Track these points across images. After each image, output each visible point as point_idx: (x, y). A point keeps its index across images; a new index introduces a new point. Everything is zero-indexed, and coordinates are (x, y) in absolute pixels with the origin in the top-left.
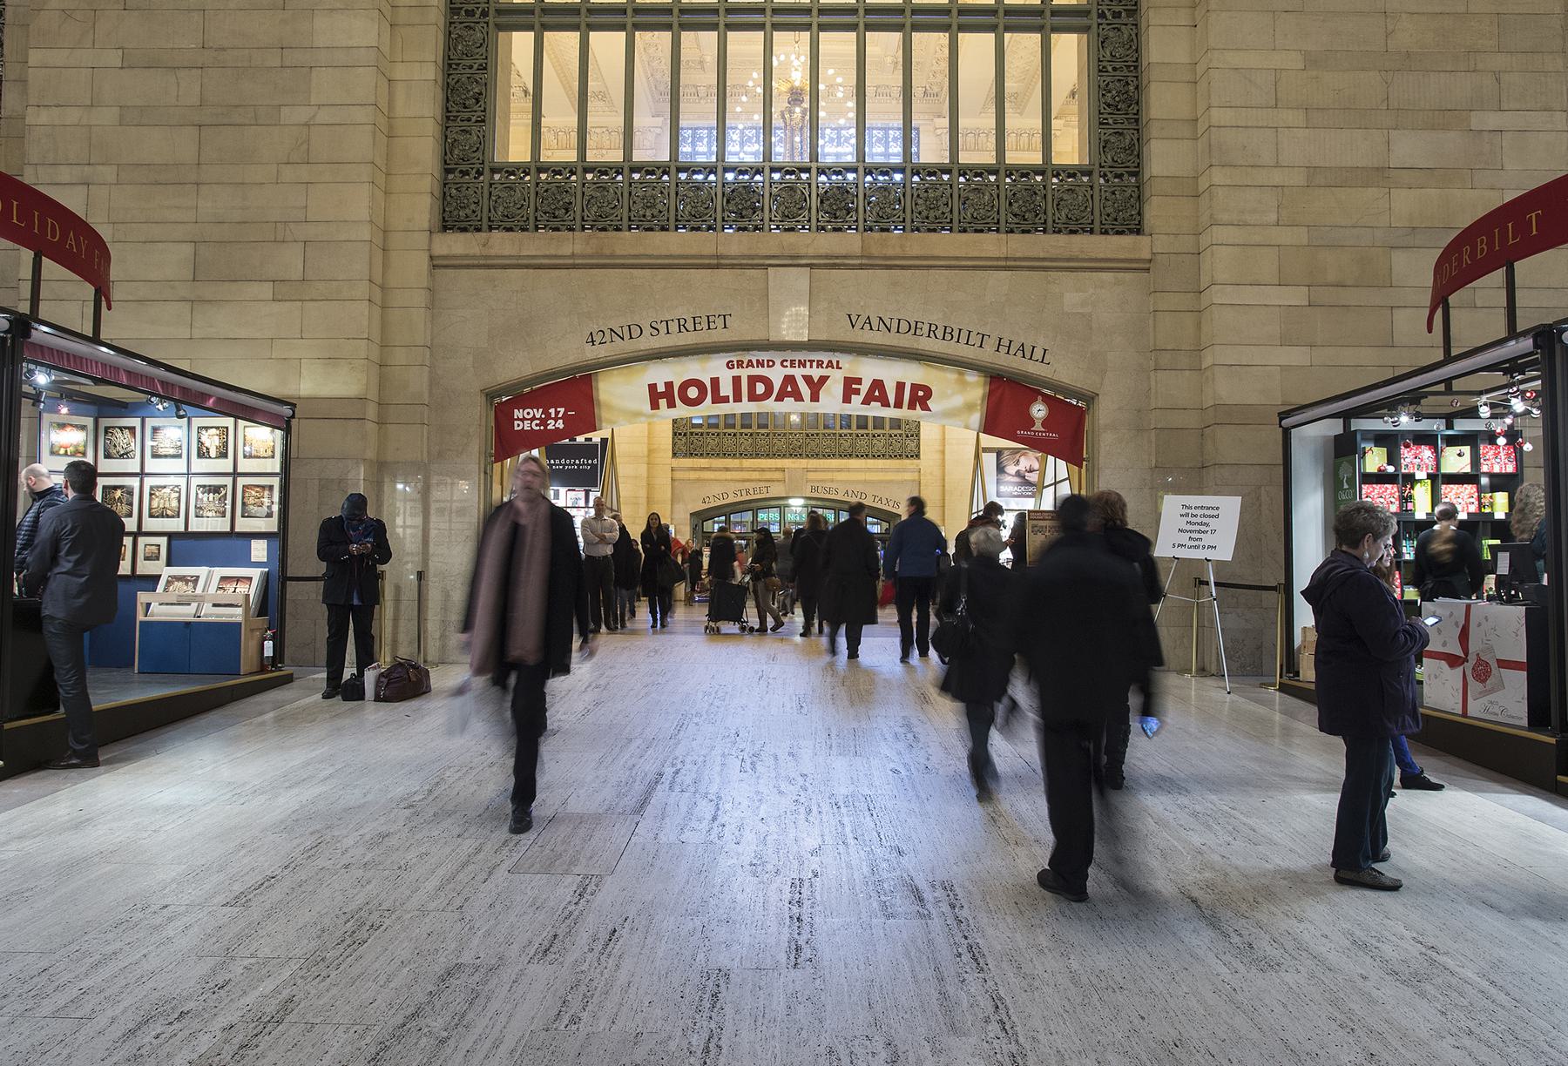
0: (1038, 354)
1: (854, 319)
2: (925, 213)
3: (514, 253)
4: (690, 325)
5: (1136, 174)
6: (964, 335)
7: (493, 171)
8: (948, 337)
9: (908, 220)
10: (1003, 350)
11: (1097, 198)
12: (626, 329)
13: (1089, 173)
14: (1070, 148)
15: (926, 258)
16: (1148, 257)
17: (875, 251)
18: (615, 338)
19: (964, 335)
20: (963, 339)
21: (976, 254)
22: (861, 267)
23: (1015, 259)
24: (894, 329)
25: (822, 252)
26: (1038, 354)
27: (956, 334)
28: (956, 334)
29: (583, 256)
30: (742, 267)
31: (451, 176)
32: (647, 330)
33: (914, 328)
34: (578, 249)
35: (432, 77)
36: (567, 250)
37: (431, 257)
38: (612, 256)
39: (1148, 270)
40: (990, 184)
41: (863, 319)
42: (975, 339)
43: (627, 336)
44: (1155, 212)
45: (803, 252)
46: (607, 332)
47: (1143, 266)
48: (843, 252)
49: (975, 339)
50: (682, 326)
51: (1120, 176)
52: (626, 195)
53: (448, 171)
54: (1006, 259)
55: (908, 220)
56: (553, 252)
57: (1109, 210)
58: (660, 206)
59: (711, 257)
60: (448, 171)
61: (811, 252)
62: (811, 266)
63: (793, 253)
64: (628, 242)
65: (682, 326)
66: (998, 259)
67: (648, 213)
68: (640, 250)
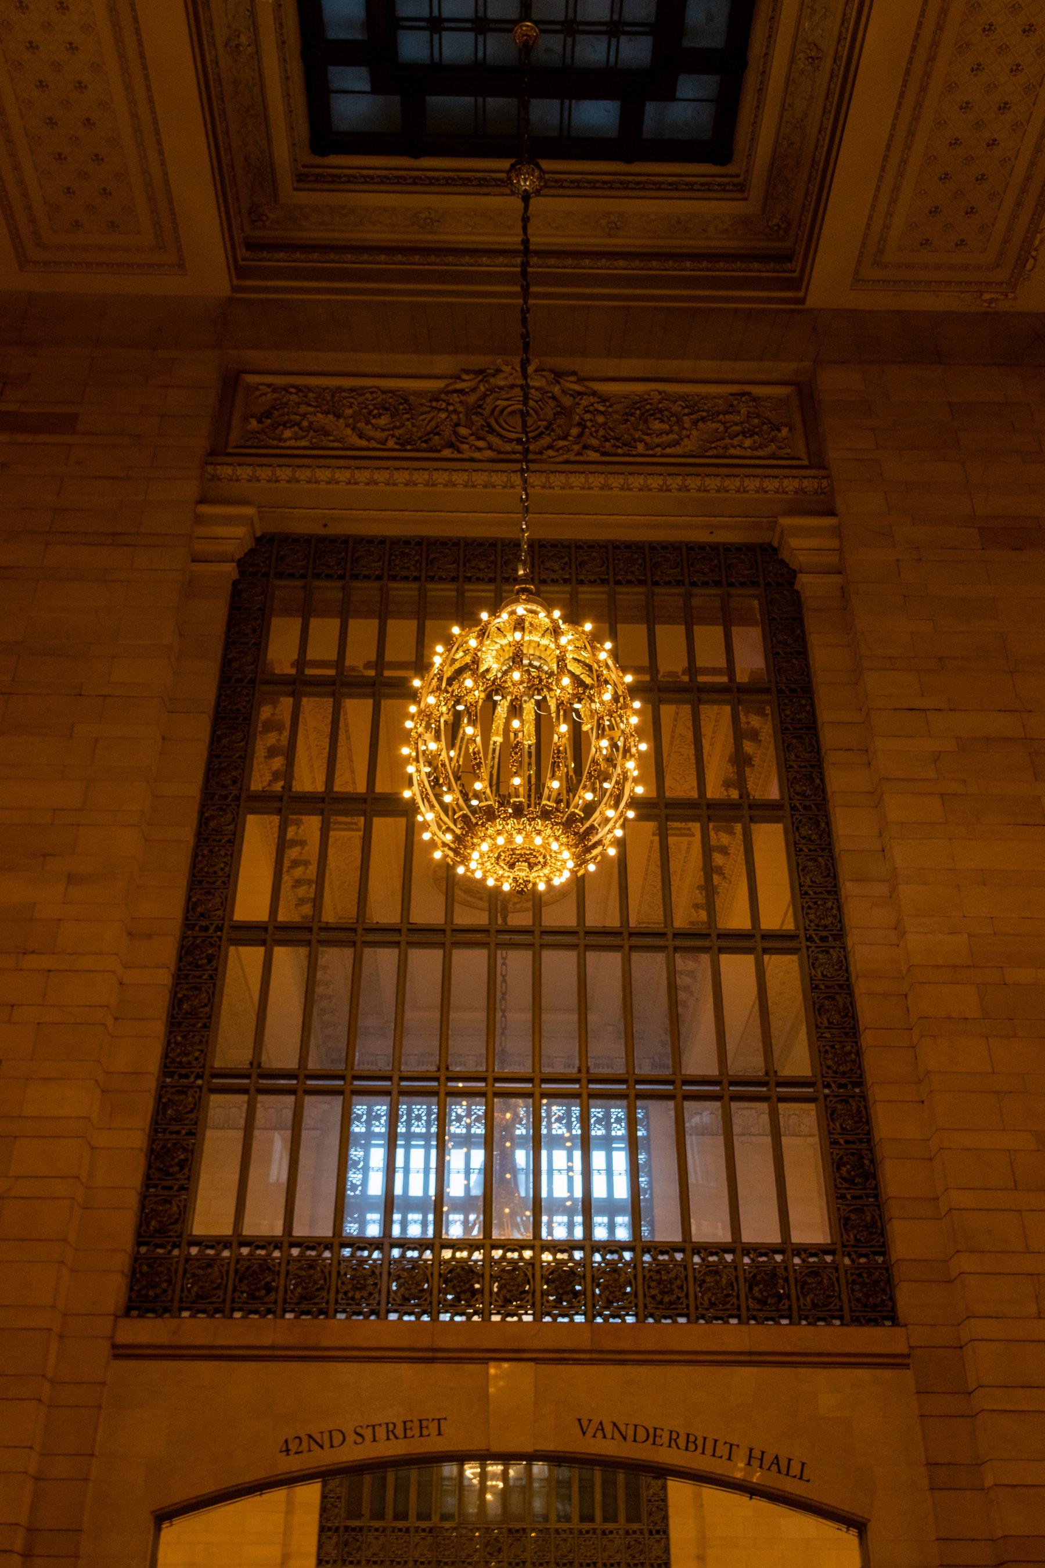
0: (795, 1469)
1: (585, 1424)
2: (659, 1298)
3: (207, 1342)
4: (399, 1431)
5: (883, 1254)
6: (709, 1444)
7: (191, 1244)
8: (692, 1447)
9: (641, 1305)
10: (755, 1463)
11: (843, 1281)
12: (326, 1435)
13: (832, 1252)
14: (811, 1226)
15: (661, 1352)
16: (906, 1351)
18: (314, 1446)
19: (709, 1444)
20: (709, 1450)
22: (591, 1362)
23: (760, 1354)
24: (630, 1437)
25: (549, 1345)
26: (795, 1469)
27: (700, 1442)
28: (700, 1442)
30: (460, 1360)
31: (143, 1250)
32: (351, 1437)
33: (653, 1436)
34: (281, 1339)
36: (266, 1340)
37: (114, 1346)
39: (907, 1366)
40: (726, 1265)
41: (595, 1424)
42: (723, 1450)
43: (327, 1445)
44: (906, 1297)
45: (526, 1345)
46: (305, 1439)
47: (896, 1362)
48: (570, 1345)
49: (723, 1450)
50: (391, 1434)
51: (866, 1256)
52: (334, 1274)
53: (139, 1244)
55: (641, 1305)
57: (859, 1295)
58: (370, 1288)
59: (426, 1350)
60: (139, 1244)
61: (536, 1344)
63: (515, 1345)
65: (391, 1434)
66: (741, 1353)
68: (347, 1342)
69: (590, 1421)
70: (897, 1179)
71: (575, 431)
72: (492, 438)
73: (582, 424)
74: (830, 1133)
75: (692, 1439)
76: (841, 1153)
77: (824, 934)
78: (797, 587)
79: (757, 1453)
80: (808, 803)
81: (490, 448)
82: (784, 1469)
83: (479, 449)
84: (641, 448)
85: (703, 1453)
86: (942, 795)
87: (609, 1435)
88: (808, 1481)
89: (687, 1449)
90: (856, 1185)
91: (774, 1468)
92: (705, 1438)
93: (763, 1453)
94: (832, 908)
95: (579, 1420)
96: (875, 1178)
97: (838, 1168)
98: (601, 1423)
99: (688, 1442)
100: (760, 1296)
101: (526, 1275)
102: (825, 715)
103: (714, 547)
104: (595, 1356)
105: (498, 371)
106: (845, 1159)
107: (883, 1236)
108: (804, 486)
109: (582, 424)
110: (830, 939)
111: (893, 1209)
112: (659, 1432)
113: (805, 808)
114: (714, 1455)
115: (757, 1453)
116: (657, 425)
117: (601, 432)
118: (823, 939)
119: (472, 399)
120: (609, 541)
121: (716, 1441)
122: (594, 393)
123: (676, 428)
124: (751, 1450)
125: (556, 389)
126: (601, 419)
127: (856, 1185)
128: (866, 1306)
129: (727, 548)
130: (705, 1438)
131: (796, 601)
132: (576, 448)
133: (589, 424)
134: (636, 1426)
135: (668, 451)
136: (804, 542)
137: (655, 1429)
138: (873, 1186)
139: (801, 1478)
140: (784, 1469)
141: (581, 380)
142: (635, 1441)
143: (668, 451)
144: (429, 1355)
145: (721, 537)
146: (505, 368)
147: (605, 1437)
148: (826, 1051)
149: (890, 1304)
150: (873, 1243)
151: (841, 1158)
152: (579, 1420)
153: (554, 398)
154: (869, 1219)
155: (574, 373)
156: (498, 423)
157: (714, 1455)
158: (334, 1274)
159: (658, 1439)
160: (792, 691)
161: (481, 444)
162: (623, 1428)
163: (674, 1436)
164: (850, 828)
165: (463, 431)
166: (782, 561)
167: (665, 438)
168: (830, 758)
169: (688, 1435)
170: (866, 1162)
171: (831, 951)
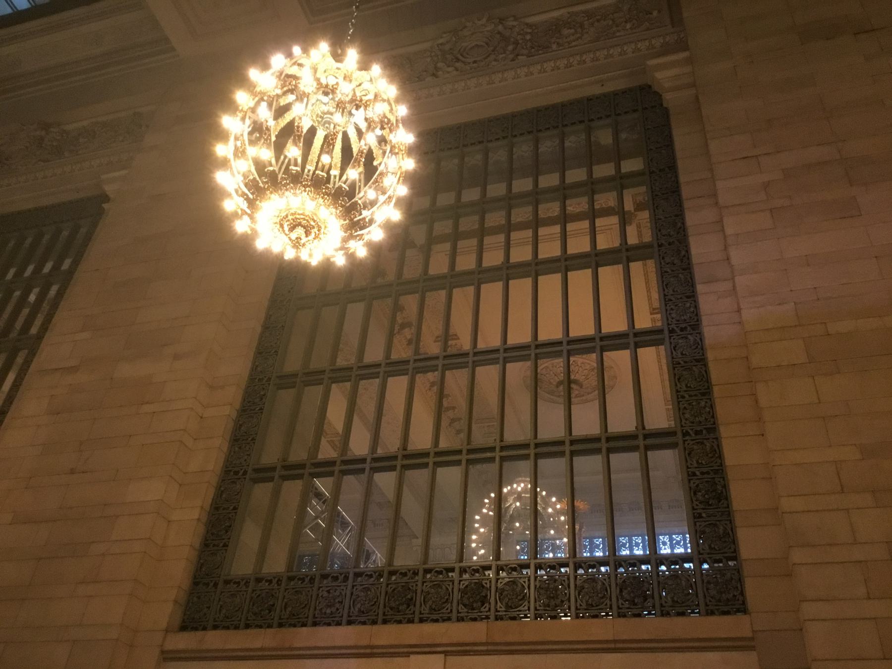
5: (734, 558)
17: (498, 638)
21: (585, 638)
22: (488, 653)
25: (455, 641)
29: (270, 649)
35: (196, 517)
36: (258, 644)
38: (291, 649)
44: (752, 589)
54: (615, 641)
56: (247, 646)
61: (445, 641)
62: (446, 653)
64: (304, 636)
67: (328, 611)
70: (742, 496)
71: (510, 48)
72: (458, 65)
73: (516, 43)
74: (688, 467)
76: (697, 482)
77: (683, 326)
78: (665, 105)
80: (671, 241)
81: (457, 70)
83: (448, 72)
84: (554, 47)
86: (771, 210)
90: (711, 505)
94: (690, 307)
96: (727, 499)
97: (695, 494)
100: (628, 598)
101: (447, 589)
102: (682, 179)
103: (605, 95)
104: (490, 648)
105: (465, 27)
106: (701, 486)
107: (734, 543)
108: (667, 40)
109: (516, 43)
110: (689, 328)
111: (738, 520)
113: (670, 244)
116: (566, 32)
117: (529, 44)
118: (682, 330)
119: (447, 47)
120: (534, 108)
122: (527, 24)
123: (579, 30)
125: (500, 28)
126: (528, 37)
127: (711, 505)
128: (719, 601)
129: (615, 94)
131: (666, 113)
132: (511, 56)
133: (520, 42)
135: (574, 44)
136: (667, 74)
138: (725, 505)
141: (516, 19)
143: (574, 44)
144: (368, 651)
145: (610, 87)
146: (468, 24)
148: (685, 408)
149: (741, 598)
150: (726, 550)
151: (697, 486)
153: (499, 33)
154: (721, 531)
155: (514, 16)
156: (462, 55)
158: (314, 597)
160: (660, 171)
161: (450, 69)
164: (702, 249)
165: (440, 65)
166: (655, 92)
167: (572, 38)
168: (687, 204)
170: (719, 487)
171: (689, 336)
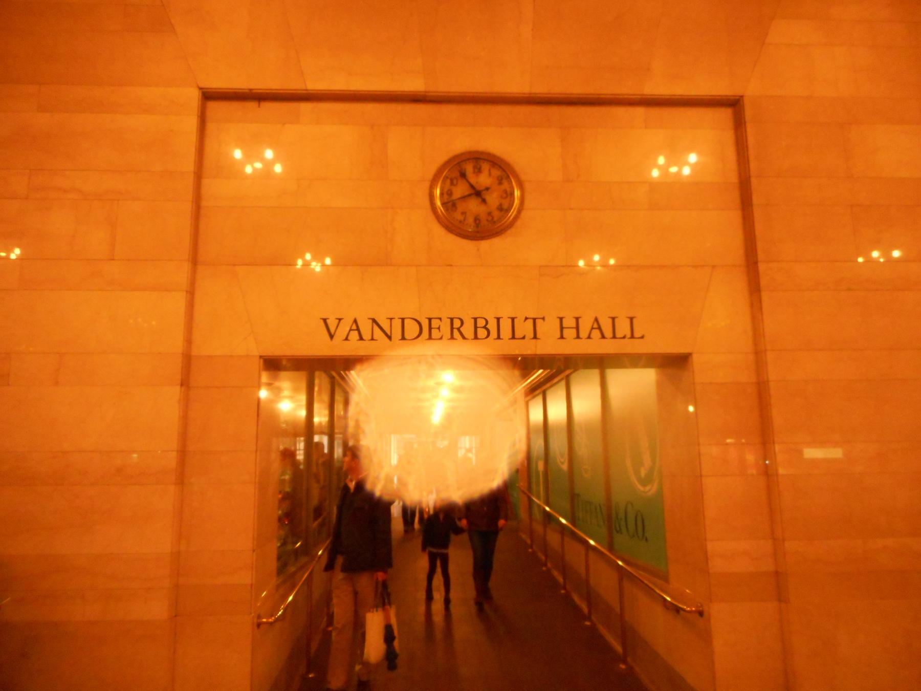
0: (623, 328)
1: (332, 324)
6: (506, 326)
8: (482, 333)
19: (506, 326)
26: (623, 328)
27: (492, 326)
28: (492, 326)
49: (525, 329)
69: (340, 320)
75: (481, 323)
79: (569, 322)
82: (608, 333)
85: (499, 337)
87: (366, 335)
88: (642, 337)
89: (476, 337)
91: (596, 334)
92: (498, 319)
93: (577, 319)
95: (325, 320)
98: (355, 321)
99: (476, 327)
112: (435, 323)
114: (513, 337)
115: (569, 322)
121: (513, 319)
124: (561, 319)
130: (498, 319)
134: (403, 320)
137: (430, 320)
139: (632, 337)
140: (608, 333)
142: (403, 338)
147: (361, 338)
152: (325, 320)
157: (513, 337)
159: (434, 332)
162: (386, 325)
163: (457, 324)
169: (475, 319)
